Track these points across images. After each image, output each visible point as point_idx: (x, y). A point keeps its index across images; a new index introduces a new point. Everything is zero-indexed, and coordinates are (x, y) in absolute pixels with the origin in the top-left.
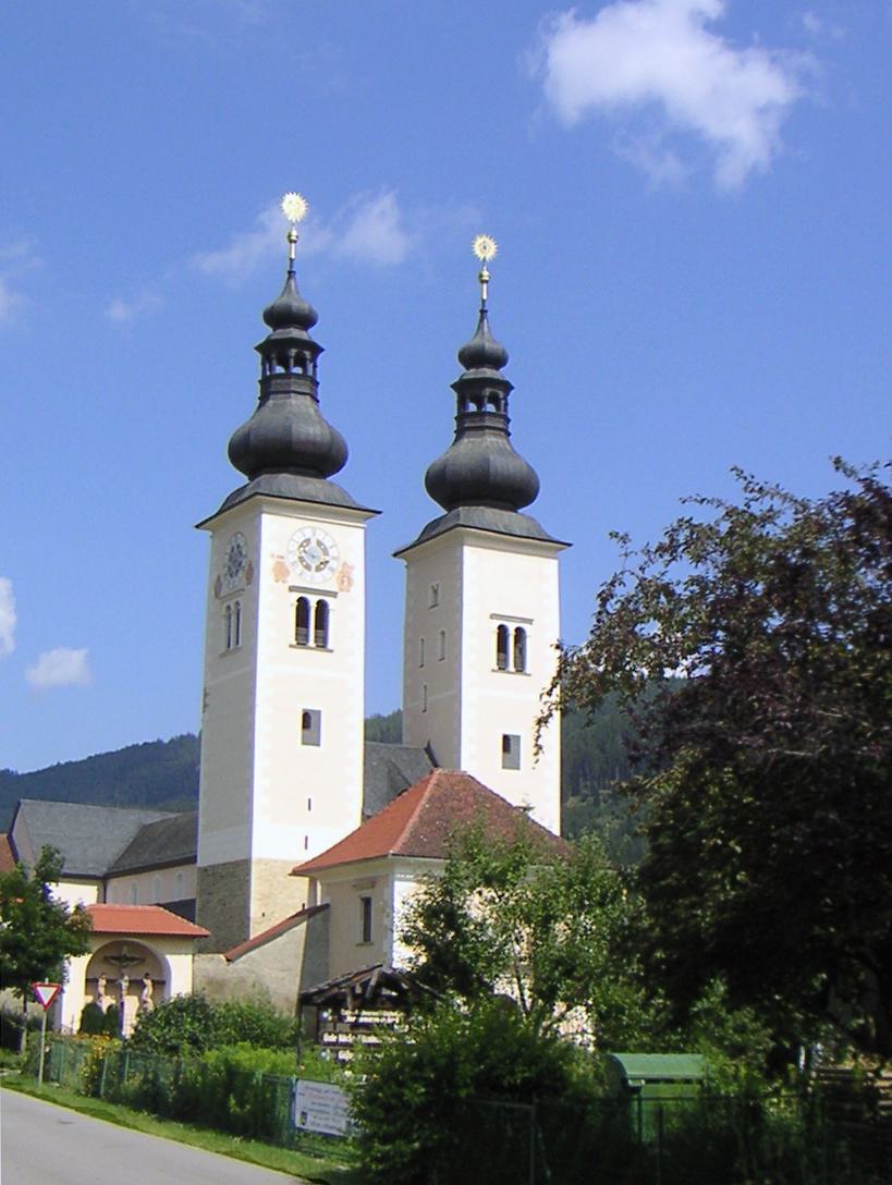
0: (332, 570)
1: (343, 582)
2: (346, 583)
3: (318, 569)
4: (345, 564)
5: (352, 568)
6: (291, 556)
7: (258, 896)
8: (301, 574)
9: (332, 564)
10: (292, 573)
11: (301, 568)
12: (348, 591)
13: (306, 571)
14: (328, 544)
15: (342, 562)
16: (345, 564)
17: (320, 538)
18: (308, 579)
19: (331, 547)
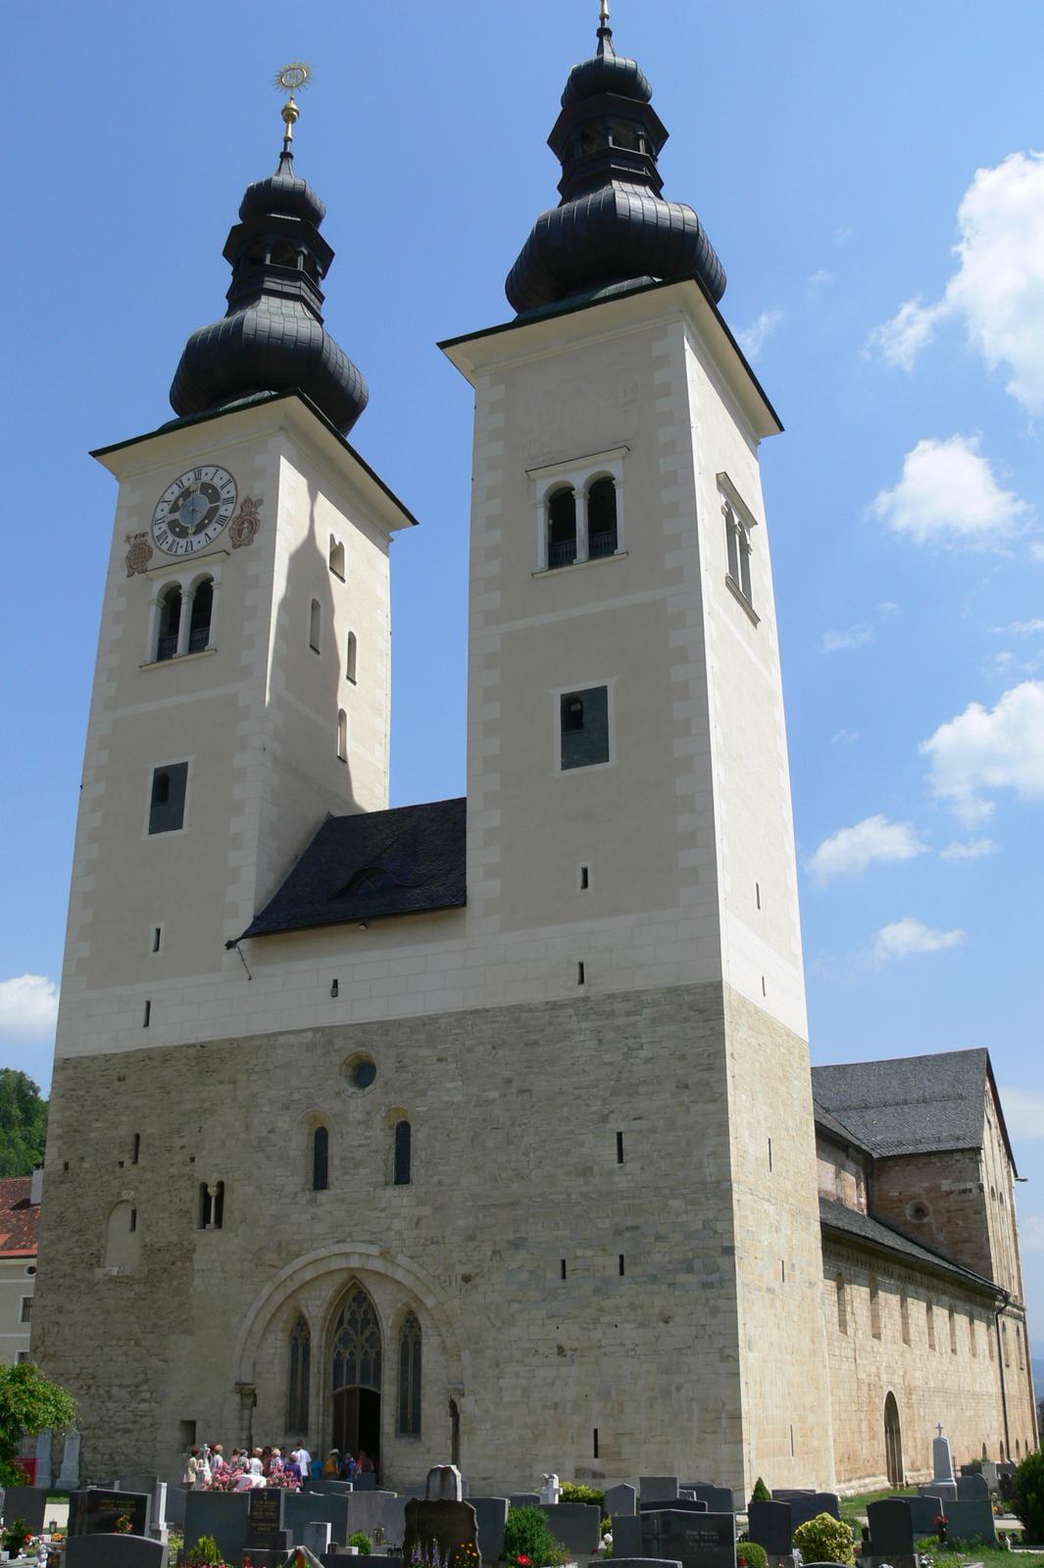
0: (223, 520)
1: (240, 536)
2: (245, 531)
3: (200, 528)
4: (248, 501)
5: (261, 502)
6: (156, 528)
7: (59, 1132)
8: (170, 549)
9: (222, 512)
10: (155, 551)
11: (171, 538)
12: (250, 542)
13: (176, 539)
14: (217, 483)
15: (241, 500)
16: (248, 501)
17: (205, 479)
18: (181, 551)
19: (222, 487)
